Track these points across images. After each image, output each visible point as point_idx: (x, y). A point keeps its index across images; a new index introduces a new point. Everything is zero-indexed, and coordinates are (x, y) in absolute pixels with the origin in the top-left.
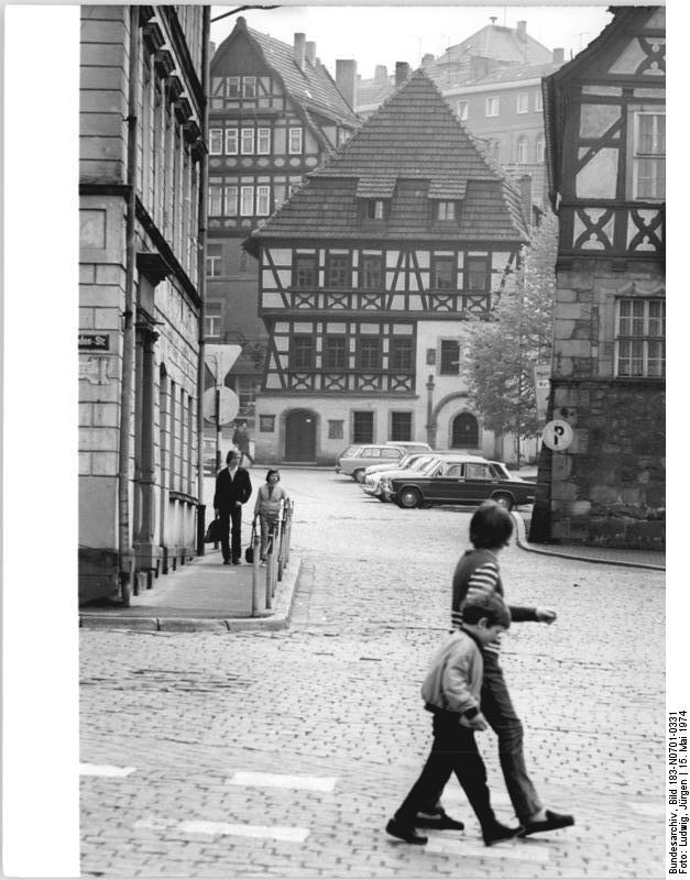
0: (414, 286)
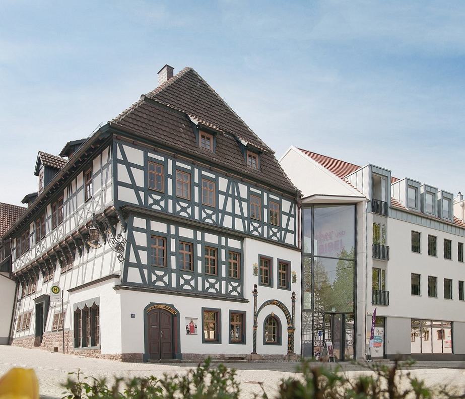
0: (238, 212)
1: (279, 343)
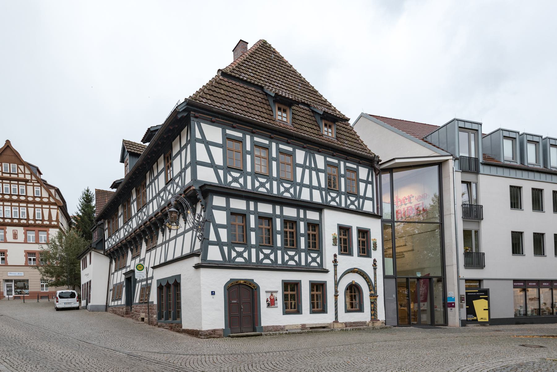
0: (315, 183)
1: (361, 310)
